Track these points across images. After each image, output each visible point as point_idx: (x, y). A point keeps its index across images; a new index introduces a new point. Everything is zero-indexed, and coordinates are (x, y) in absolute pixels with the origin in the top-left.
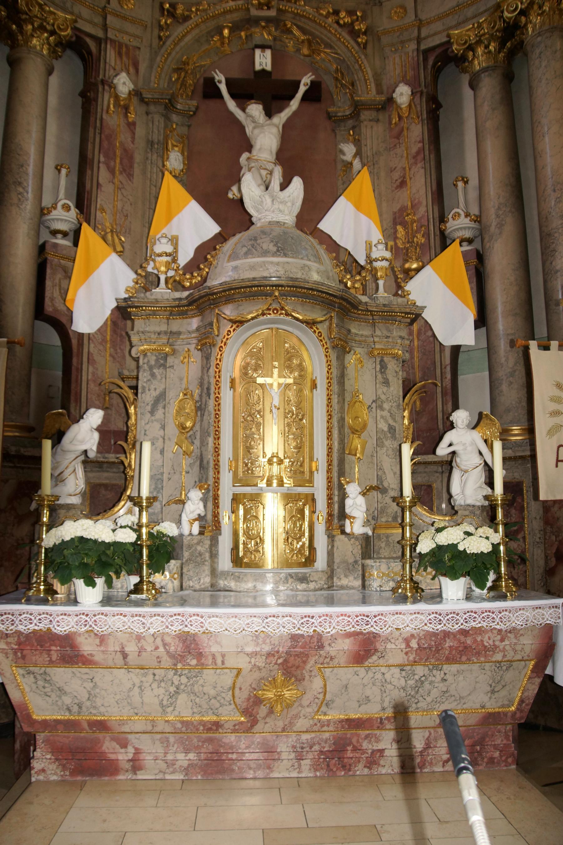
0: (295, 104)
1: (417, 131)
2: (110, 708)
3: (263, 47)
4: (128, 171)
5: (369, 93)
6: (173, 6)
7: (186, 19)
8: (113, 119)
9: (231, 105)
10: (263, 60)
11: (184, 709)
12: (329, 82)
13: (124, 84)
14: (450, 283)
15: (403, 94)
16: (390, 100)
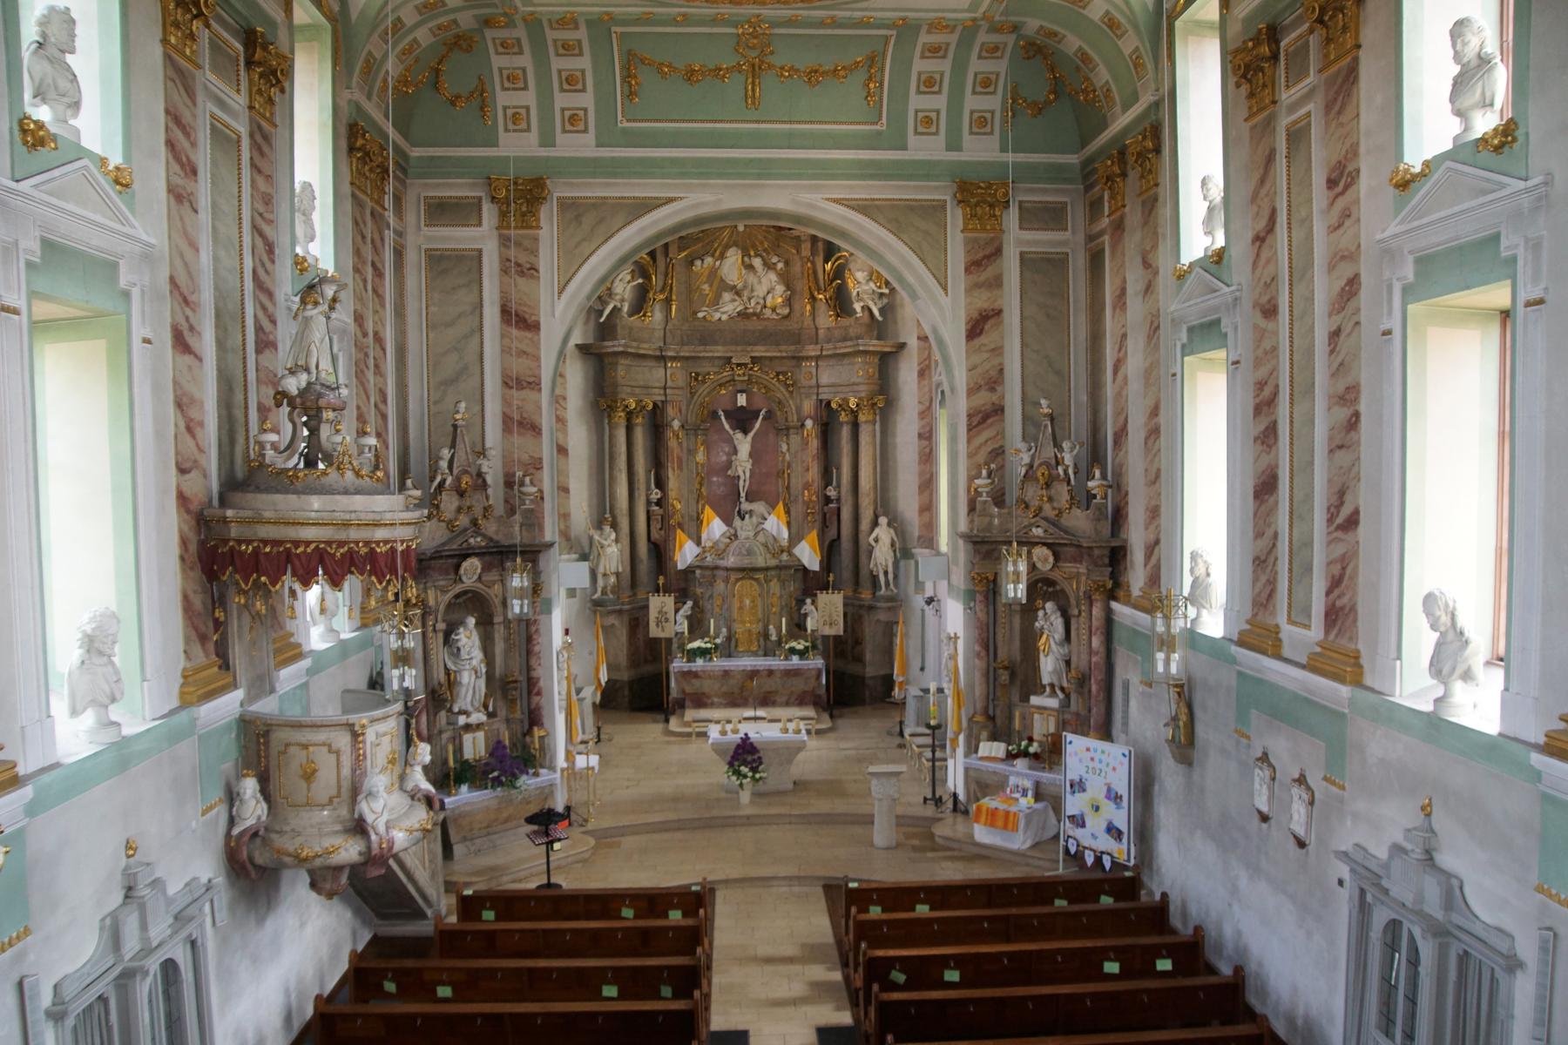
0: (757, 425)
1: (814, 444)
2: (706, 690)
3: (742, 391)
4: (680, 468)
5: (793, 419)
6: (697, 374)
7: (704, 382)
8: (673, 443)
9: (727, 427)
10: (742, 400)
11: (724, 689)
12: (775, 407)
13: (676, 424)
14: (812, 547)
15: (809, 423)
16: (803, 425)
